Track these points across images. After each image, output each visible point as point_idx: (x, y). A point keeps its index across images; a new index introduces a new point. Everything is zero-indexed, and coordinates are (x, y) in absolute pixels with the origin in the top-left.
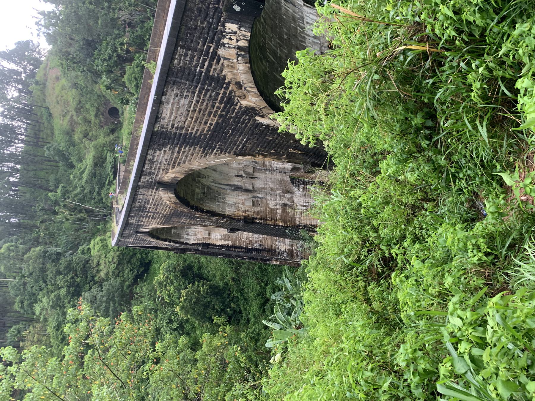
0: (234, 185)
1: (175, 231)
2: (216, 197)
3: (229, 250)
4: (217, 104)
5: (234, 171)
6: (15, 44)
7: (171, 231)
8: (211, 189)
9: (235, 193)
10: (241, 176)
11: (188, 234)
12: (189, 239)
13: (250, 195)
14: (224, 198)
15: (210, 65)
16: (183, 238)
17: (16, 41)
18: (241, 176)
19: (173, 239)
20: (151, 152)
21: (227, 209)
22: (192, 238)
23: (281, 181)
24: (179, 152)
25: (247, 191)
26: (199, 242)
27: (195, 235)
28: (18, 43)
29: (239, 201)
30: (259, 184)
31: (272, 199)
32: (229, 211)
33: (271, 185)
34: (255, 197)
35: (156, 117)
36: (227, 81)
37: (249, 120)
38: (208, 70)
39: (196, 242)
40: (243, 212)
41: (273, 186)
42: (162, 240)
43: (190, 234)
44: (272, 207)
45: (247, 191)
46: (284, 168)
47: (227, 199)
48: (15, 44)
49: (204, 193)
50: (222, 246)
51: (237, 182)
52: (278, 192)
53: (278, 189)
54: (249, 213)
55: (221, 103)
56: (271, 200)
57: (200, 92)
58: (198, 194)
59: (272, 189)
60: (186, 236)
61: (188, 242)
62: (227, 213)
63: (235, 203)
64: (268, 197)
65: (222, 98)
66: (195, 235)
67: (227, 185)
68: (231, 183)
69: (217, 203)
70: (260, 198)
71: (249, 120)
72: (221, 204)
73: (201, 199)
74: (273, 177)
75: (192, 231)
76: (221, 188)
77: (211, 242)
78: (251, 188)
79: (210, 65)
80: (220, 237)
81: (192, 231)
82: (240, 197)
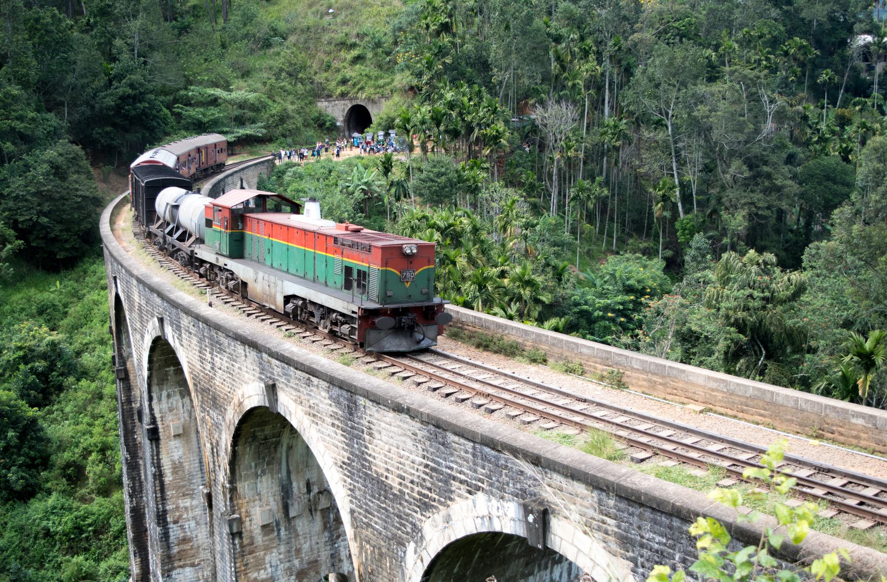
0: (291, 483)
1: (171, 373)
2: (264, 458)
3: (155, 479)
4: (416, 489)
5: (315, 475)
7: (169, 366)
8: (275, 448)
9: (276, 488)
10: (309, 491)
11: (169, 396)
12: (160, 400)
13: (280, 515)
14: (264, 472)
15: (461, 482)
16: (161, 390)
18: (309, 491)
19: (154, 373)
20: (324, 384)
21: (246, 484)
22: (165, 405)
23: (316, 561)
24: (333, 425)
25: (286, 508)
26: (158, 420)
27: (171, 410)
29: (264, 499)
30: (301, 525)
31: (282, 556)
32: (243, 487)
33: (306, 547)
34: (278, 524)
35: (377, 400)
36: (449, 502)
37: (407, 533)
38: (454, 478)
39: (158, 415)
40: (247, 512)
41: (303, 551)
42: (150, 357)
43: (171, 400)
44: (267, 558)
45: (286, 508)
46: (340, 561)
47: (264, 479)
49: (266, 439)
50: (158, 466)
51: (298, 486)
52: (296, 562)
53: (301, 562)
54: (247, 524)
55: (420, 493)
56: (280, 554)
57: (427, 466)
58: (263, 431)
59: (298, 551)
60: (164, 393)
61: (155, 401)
62: (239, 485)
63: (259, 494)
64: (283, 549)
65: (427, 497)
66: (171, 410)
67: (289, 472)
68: (293, 477)
69: (253, 464)
70: (279, 534)
71: (407, 533)
72: (253, 470)
73: (254, 437)
74: (322, 545)
75: (177, 401)
76: (280, 464)
77: (162, 442)
78: (292, 514)
79: (461, 482)
80: (176, 458)
81: (177, 401)
82: (271, 499)
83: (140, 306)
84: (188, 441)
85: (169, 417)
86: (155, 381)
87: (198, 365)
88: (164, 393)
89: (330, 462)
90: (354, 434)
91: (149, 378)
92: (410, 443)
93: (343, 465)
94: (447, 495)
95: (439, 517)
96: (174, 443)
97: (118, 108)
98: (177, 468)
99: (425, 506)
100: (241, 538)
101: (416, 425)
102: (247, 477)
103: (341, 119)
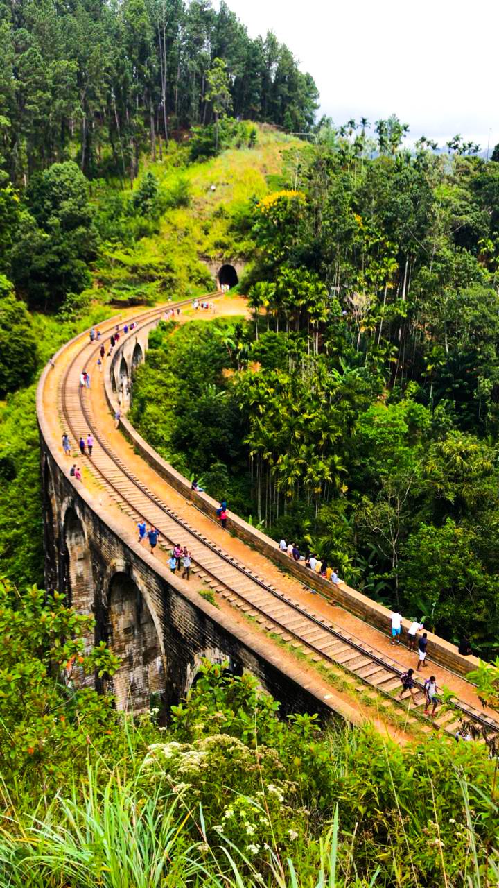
6: (308, 74)
11: (76, 536)
14: (126, 600)
15: (210, 641)
16: (71, 532)
17: (311, 74)
21: (116, 606)
22: (73, 541)
27: (77, 544)
28: (309, 79)
33: (149, 639)
34: (133, 627)
39: (69, 547)
44: (127, 647)
48: (308, 74)
52: (143, 649)
59: (145, 642)
60: (74, 534)
64: (135, 641)
70: (134, 634)
78: (142, 622)
80: (79, 572)
83: (61, 485)
84: (87, 563)
85: (76, 549)
86: (68, 527)
87: (93, 537)
88: (74, 534)
89: (155, 614)
90: (167, 605)
91: (65, 525)
92: (189, 617)
93: (160, 616)
94: (204, 646)
95: (201, 654)
96: (78, 564)
97: (47, 269)
98: (79, 578)
99: (196, 649)
100: (112, 636)
101: (190, 609)
102: (117, 602)
103: (215, 274)
